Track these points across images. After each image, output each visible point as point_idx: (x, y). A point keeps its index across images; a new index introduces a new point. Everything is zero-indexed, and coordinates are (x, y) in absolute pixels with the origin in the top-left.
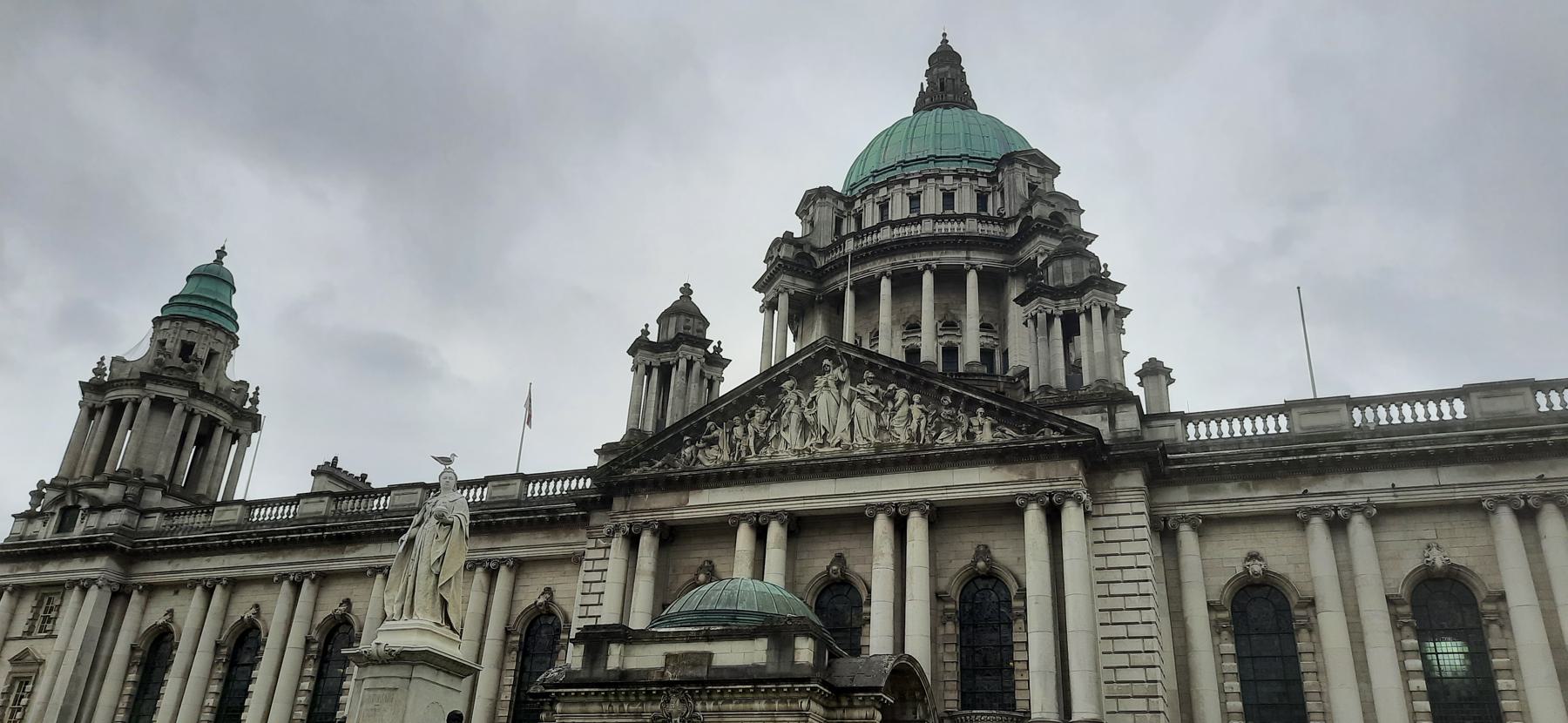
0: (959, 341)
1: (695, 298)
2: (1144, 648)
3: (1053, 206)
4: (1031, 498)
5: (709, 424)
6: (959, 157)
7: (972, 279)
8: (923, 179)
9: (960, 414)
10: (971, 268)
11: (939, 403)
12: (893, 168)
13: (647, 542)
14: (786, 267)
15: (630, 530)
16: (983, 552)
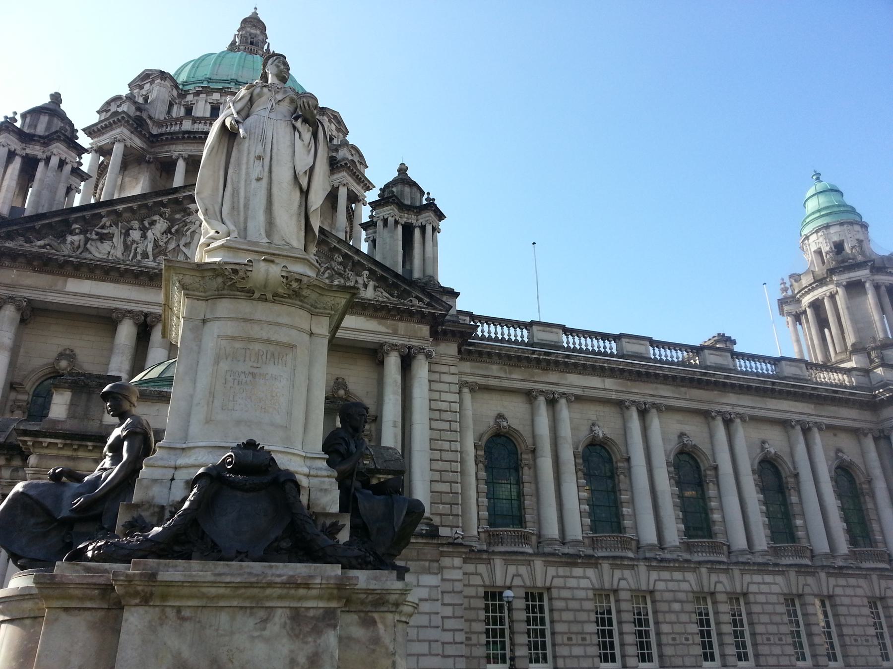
2: (451, 469)
3: (352, 155)
4: (394, 347)
5: (104, 220)
9: (348, 272)
12: (229, 82)
14: (128, 122)
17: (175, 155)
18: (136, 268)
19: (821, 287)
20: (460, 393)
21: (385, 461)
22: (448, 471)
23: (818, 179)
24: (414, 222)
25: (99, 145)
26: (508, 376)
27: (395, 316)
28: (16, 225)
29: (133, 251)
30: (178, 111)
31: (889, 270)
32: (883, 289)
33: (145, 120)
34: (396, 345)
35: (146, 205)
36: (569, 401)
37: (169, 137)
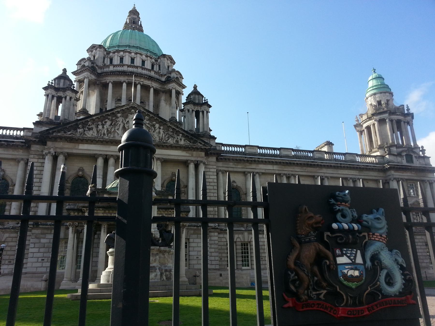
3: (177, 75)
4: (192, 161)
5: (89, 123)
6: (147, 50)
7: (152, 90)
8: (136, 53)
9: (174, 135)
10: (152, 87)
11: (168, 130)
12: (126, 46)
13: (61, 158)
15: (55, 154)
17: (108, 81)
18: (102, 139)
19: (370, 121)
20: (217, 174)
21: (184, 208)
23: (374, 72)
24: (199, 109)
26: (236, 167)
27: (192, 150)
28: (60, 127)
29: (100, 133)
30: (107, 62)
31: (397, 113)
32: (394, 121)
34: (192, 160)
35: (103, 116)
36: (259, 175)
37: (105, 74)
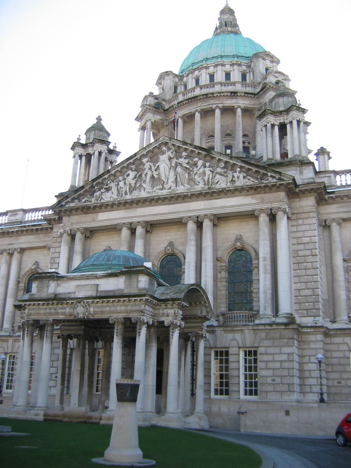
0: (233, 143)
1: (103, 123)
2: (313, 280)
3: (277, 77)
6: (233, 56)
8: (216, 66)
9: (229, 172)
10: (238, 107)
12: (202, 61)
16: (239, 239)
22: (311, 282)
25: (142, 125)
33: (161, 103)
34: (262, 210)
37: (172, 108)
